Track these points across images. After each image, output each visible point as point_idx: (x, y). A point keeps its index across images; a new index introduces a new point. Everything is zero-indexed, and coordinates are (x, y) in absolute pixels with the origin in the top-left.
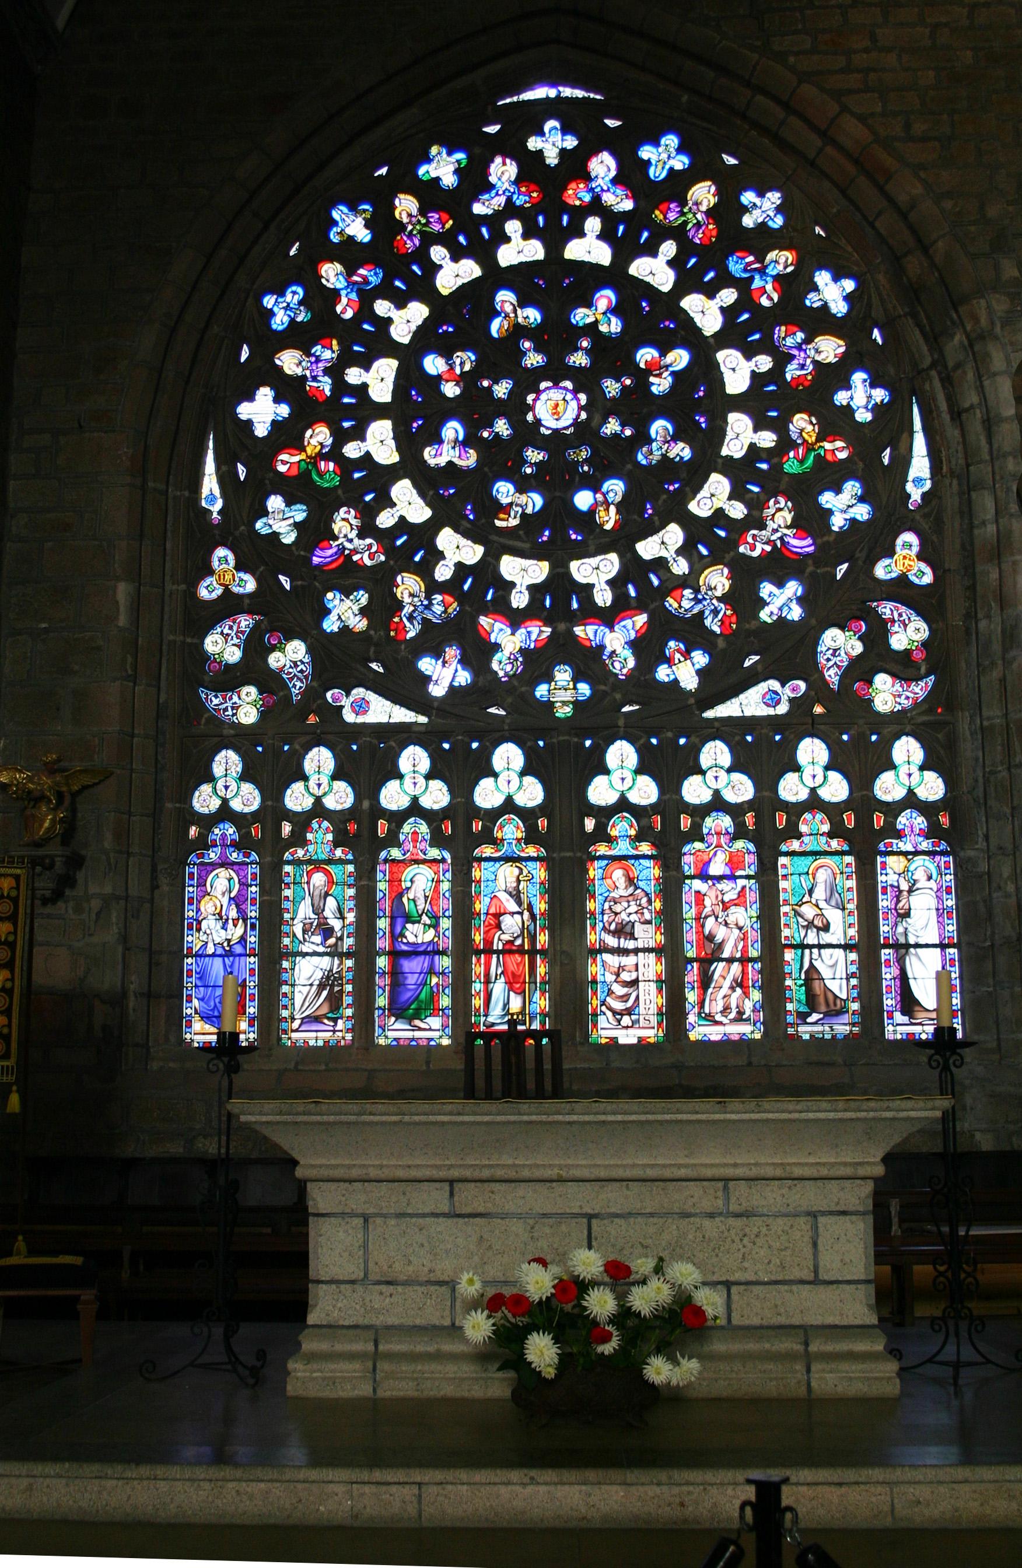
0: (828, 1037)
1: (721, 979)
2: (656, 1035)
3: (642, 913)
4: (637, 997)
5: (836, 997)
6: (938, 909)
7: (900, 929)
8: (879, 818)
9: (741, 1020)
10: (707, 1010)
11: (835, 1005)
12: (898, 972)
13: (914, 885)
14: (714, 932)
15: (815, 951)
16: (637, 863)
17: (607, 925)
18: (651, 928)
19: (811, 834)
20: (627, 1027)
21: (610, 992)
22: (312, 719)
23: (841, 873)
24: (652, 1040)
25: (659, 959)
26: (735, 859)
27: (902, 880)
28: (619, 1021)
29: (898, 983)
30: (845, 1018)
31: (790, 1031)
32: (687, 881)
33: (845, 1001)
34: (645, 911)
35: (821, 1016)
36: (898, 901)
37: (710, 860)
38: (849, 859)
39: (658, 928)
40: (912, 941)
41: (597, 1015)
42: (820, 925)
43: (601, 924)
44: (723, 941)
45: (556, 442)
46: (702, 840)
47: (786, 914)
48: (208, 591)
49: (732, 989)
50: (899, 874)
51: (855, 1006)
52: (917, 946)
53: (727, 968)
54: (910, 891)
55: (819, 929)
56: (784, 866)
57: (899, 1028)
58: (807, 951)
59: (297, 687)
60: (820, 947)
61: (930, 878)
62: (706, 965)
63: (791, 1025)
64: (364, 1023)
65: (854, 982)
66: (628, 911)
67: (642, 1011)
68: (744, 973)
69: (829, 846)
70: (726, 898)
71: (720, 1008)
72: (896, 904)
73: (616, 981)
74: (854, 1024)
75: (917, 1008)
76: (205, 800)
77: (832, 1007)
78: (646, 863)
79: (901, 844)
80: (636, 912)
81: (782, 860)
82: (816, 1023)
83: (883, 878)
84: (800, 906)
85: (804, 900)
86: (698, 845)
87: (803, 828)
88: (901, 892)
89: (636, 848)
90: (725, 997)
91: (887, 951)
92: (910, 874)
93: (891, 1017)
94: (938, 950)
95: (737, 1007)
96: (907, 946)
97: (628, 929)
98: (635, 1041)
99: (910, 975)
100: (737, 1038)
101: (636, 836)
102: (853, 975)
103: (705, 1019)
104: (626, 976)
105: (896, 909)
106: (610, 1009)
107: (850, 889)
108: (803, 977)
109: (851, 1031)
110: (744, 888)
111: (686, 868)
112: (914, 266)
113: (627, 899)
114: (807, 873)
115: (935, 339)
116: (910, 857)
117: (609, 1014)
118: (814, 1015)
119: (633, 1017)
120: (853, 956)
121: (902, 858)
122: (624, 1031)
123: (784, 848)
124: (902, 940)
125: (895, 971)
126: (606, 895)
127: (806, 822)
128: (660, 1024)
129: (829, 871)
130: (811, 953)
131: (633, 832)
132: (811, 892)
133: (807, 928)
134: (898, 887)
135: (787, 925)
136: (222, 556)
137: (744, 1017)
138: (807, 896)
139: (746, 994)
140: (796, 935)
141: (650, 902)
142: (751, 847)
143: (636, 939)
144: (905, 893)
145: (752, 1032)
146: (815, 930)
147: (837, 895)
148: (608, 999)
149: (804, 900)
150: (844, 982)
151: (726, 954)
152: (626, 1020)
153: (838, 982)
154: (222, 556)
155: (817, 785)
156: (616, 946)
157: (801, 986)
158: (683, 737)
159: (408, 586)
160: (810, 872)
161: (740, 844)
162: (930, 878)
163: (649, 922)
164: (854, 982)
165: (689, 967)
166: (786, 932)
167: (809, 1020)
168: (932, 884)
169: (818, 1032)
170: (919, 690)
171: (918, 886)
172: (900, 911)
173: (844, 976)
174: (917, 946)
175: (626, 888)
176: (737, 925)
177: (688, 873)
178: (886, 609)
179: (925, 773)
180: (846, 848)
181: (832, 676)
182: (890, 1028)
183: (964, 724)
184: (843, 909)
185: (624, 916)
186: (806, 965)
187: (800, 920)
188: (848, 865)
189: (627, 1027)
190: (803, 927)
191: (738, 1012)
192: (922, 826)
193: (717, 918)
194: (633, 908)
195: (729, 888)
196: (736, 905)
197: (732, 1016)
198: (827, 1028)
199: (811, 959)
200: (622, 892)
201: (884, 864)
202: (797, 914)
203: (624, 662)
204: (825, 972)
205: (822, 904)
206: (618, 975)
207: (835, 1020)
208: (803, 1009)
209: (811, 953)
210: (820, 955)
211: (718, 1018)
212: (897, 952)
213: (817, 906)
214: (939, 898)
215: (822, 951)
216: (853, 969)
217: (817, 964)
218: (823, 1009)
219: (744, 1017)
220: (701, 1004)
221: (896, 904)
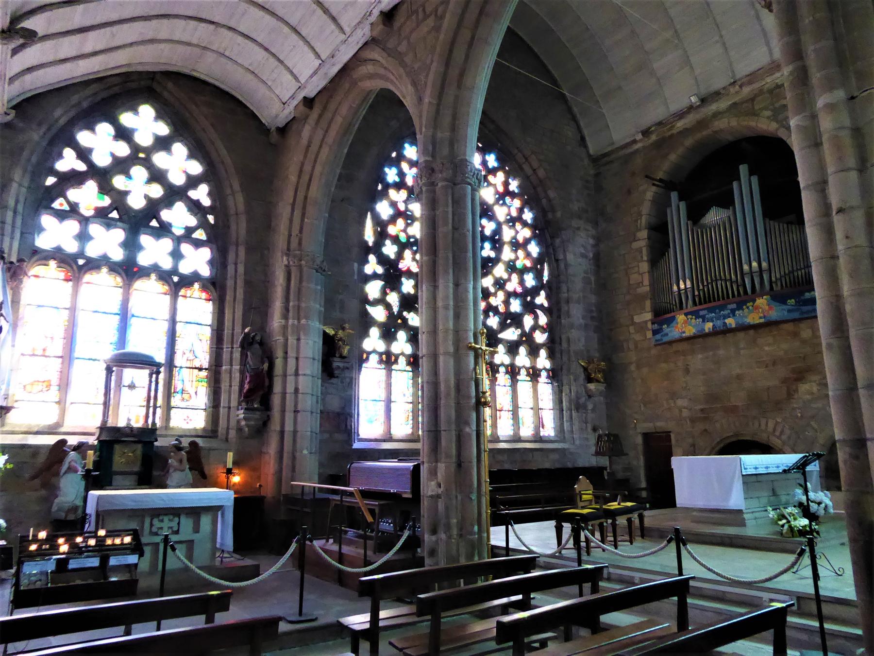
22: (399, 321)
59: (396, 309)
136: (372, 258)
154: (372, 258)
183: (557, 349)
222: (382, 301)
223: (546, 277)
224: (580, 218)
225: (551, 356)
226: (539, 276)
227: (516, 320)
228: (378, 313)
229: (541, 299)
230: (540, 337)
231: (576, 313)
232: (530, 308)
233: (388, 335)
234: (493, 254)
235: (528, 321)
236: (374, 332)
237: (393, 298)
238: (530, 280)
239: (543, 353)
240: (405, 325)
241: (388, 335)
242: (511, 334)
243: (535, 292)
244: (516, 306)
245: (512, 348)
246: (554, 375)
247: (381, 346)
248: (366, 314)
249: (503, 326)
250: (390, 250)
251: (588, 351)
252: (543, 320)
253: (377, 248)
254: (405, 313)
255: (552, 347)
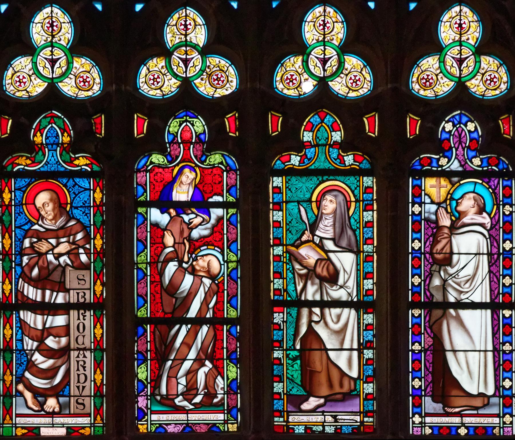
0: (329, 430)
1: (185, 349)
2: (92, 425)
3: (78, 254)
4: (68, 373)
5: (343, 374)
6: (490, 254)
7: (437, 282)
8: (413, 123)
9: (212, 405)
10: (164, 391)
11: (341, 385)
12: (430, 341)
13: (459, 219)
14: (177, 281)
15: (317, 310)
16: (71, 183)
17: (26, 269)
18: (88, 276)
19: (317, 145)
20: (52, 414)
21: (31, 366)
23: (357, 201)
24: (87, 432)
25: (98, 320)
26: (209, 179)
27: (442, 211)
28: (42, 405)
29: (430, 358)
30: (355, 405)
31: (278, 421)
32: (140, 210)
33: (355, 380)
34: (81, 251)
35: (322, 401)
36: (436, 242)
37: (174, 180)
38: (368, 181)
39: (97, 276)
40: (452, 300)
41: (11, 397)
42: (325, 273)
43: (19, 270)
44: (189, 293)
46: (162, 151)
47: (277, 258)
49: (199, 362)
50: (439, 204)
51: (369, 388)
52: (460, 305)
53: (192, 333)
54: (454, 228)
55: (322, 279)
56: (277, 190)
57: (428, 420)
58: (305, 312)
60: (323, 304)
61: (481, 210)
62: (164, 328)
63: (280, 414)
65: (369, 354)
66: (56, 251)
67: (74, 391)
68: (217, 339)
69: (343, 162)
70: (195, 234)
71: (181, 388)
72: (432, 249)
73: (38, 349)
74: (366, 414)
75: (454, 392)
77: (337, 389)
78: (84, 183)
79: (443, 161)
80: (68, 253)
81: (277, 181)
82: (313, 411)
83: (417, 209)
84: (297, 247)
85: (304, 238)
86: (157, 158)
87: (307, 136)
88: (440, 228)
89: (71, 163)
90: (188, 373)
91: (417, 312)
92: (454, 203)
93: (418, 405)
94: (489, 312)
95: (206, 387)
96: (446, 305)
97: (56, 276)
98: (62, 432)
99: (448, 346)
100: (204, 429)
101: (70, 144)
102: (368, 345)
103: (160, 403)
104: (51, 342)
105: (431, 253)
106: (30, 387)
107: (369, 224)
108: (298, 347)
109: (362, 422)
110: (220, 219)
111: (140, 190)
113: (56, 234)
114: (310, 201)
116: (455, 179)
117: (28, 395)
118: (312, 399)
119: (61, 399)
120: (369, 319)
121: (443, 182)
122: (48, 420)
123: (278, 164)
124: (438, 297)
125: (426, 340)
126: (26, 227)
127: (310, 128)
128: (98, 411)
129: (341, 198)
130: (311, 313)
131: (66, 139)
132: (313, 227)
133: (306, 278)
134: (437, 222)
135: (279, 275)
137: (215, 400)
138: (307, 233)
139: (218, 370)
140: (291, 288)
141: (87, 238)
142: (232, 161)
143: (67, 291)
144: (446, 231)
145: (226, 422)
146: (317, 281)
147: (350, 232)
148: (27, 375)
149: (304, 238)
150: (355, 354)
151: (193, 313)
152: (51, 403)
153: (345, 354)
155: (328, 73)
156: (39, 299)
157: (294, 359)
158: (139, 2)
160: (314, 199)
161: (216, 158)
162: (481, 210)
163: (86, 267)
164: (369, 354)
165: (140, 331)
166: (278, 284)
167: (305, 406)
168: (486, 220)
169: (316, 424)
171: (466, 220)
172: (439, 256)
173: (355, 346)
174: (460, 305)
175: (55, 218)
176: (208, 271)
177: (142, 198)
179: (483, 58)
180: (365, 165)
182: (417, 419)
184: (357, 253)
185: (50, 257)
186: (303, 329)
187: (297, 266)
188: (368, 190)
189: (52, 414)
190: (300, 276)
191: (205, 395)
192: (475, 135)
193: (181, 262)
194: (63, 248)
195: (198, 220)
196: (207, 244)
197: (198, 399)
198: (329, 419)
199: (310, 321)
200: (49, 224)
201: (418, 190)
202: (295, 258)
204: (330, 342)
205: (330, 245)
206: (41, 340)
207: (340, 407)
208: (297, 391)
209: (311, 313)
210: (323, 316)
211: (179, 401)
212: (429, 314)
213: (321, 246)
214: (493, 239)
215: (327, 311)
216: (369, 335)
217: (320, 329)
218: (325, 391)
219: (215, 400)
220: (156, 381)
221: (433, 246)
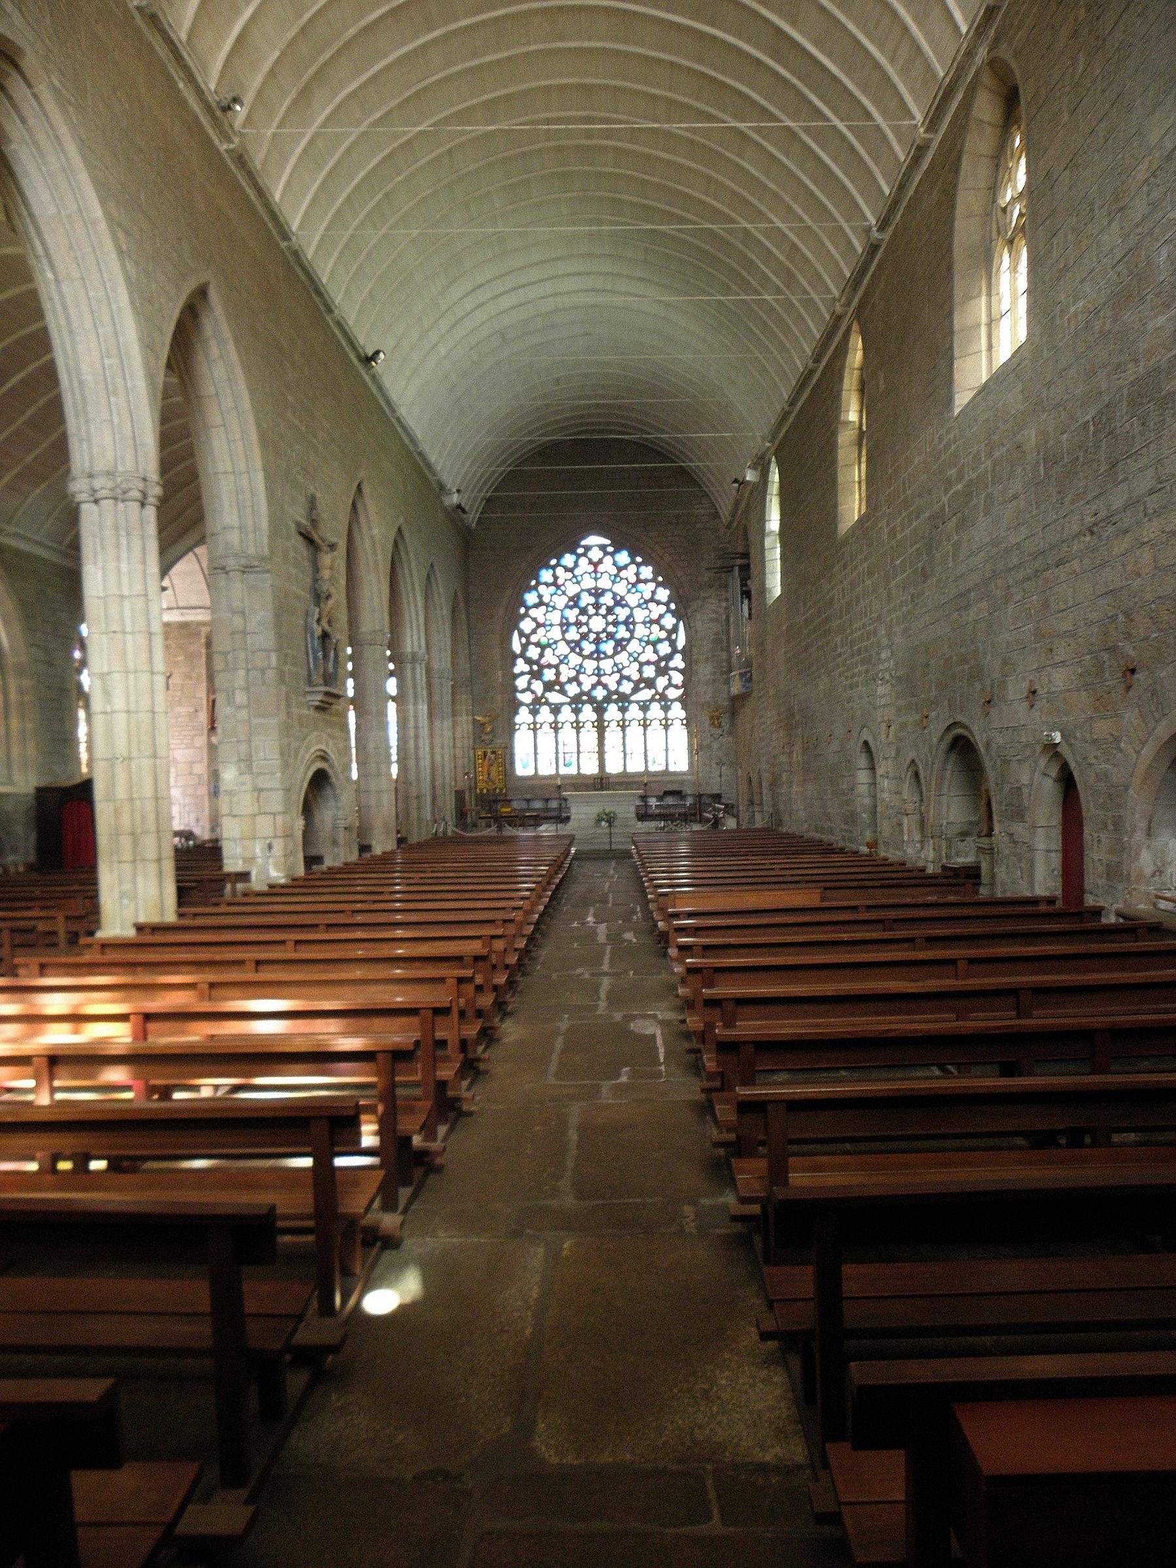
45: (598, 633)
48: (517, 670)
59: (539, 694)
64: (557, 769)
76: (518, 719)
112: (681, 591)
115: (685, 609)
136: (520, 661)
154: (520, 661)
159: (563, 668)
170: (681, 691)
178: (673, 673)
181: (660, 691)
203: (613, 687)
222: (528, 689)
223: (681, 642)
224: (710, 586)
225: (684, 707)
226: (673, 644)
227: (650, 683)
228: (526, 698)
229: (678, 661)
230: (673, 693)
231: (705, 671)
232: (662, 671)
233: (534, 712)
234: (627, 635)
235: (661, 682)
236: (524, 711)
237: (538, 686)
238: (665, 649)
239: (677, 706)
240: (547, 703)
241: (534, 712)
242: (645, 694)
243: (669, 657)
244: (649, 671)
245: (644, 707)
246: (688, 723)
247: (530, 719)
248: (515, 698)
249: (636, 690)
250: (533, 652)
251: (716, 702)
252: (678, 678)
253: (522, 655)
254: (547, 695)
255: (682, 700)
